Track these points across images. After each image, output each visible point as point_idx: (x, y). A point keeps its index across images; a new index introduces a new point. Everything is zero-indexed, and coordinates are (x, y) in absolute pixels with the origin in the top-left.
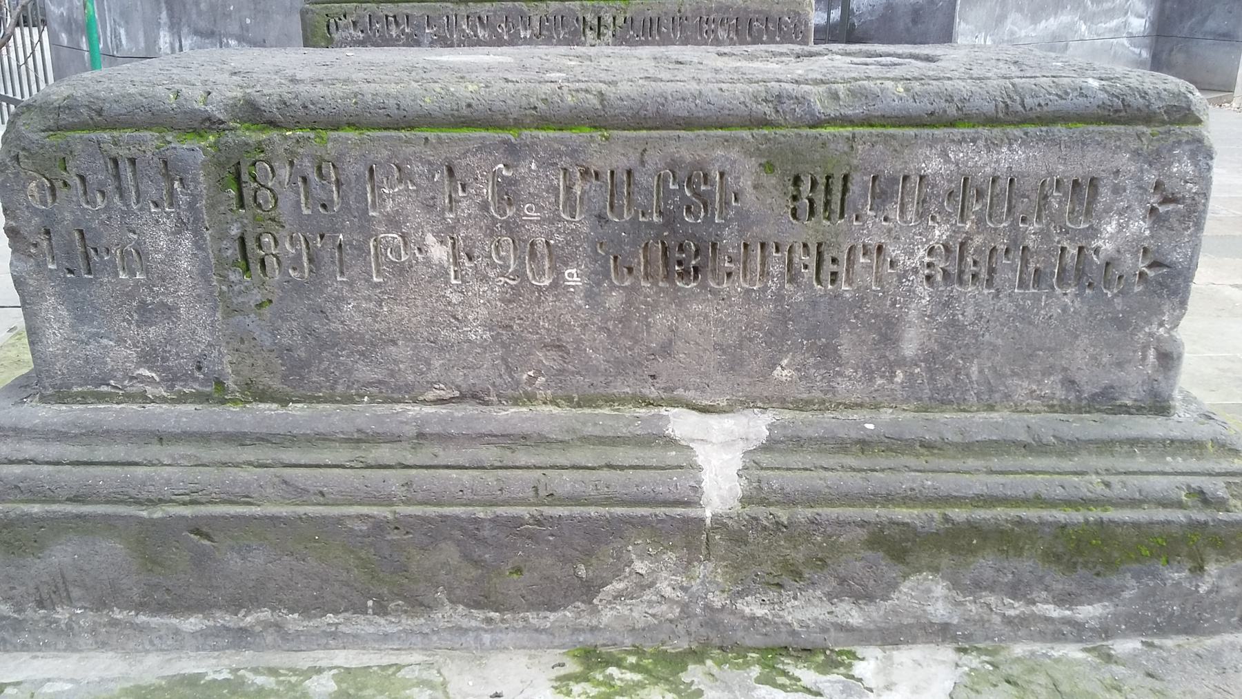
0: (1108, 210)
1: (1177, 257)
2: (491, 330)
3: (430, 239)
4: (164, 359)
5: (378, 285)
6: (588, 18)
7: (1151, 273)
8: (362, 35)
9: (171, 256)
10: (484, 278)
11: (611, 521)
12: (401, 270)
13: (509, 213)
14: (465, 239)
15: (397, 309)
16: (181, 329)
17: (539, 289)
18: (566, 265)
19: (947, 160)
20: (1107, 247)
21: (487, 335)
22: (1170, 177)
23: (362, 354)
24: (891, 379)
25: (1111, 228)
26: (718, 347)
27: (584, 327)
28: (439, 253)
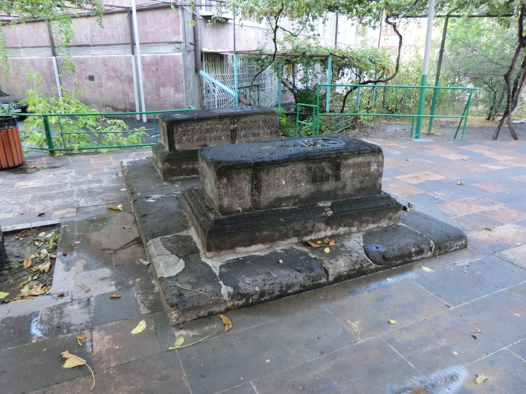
1: (381, 171)
3: (283, 181)
7: (378, 174)
9: (245, 188)
10: (290, 186)
13: (294, 175)
25: (372, 168)
28: (284, 183)
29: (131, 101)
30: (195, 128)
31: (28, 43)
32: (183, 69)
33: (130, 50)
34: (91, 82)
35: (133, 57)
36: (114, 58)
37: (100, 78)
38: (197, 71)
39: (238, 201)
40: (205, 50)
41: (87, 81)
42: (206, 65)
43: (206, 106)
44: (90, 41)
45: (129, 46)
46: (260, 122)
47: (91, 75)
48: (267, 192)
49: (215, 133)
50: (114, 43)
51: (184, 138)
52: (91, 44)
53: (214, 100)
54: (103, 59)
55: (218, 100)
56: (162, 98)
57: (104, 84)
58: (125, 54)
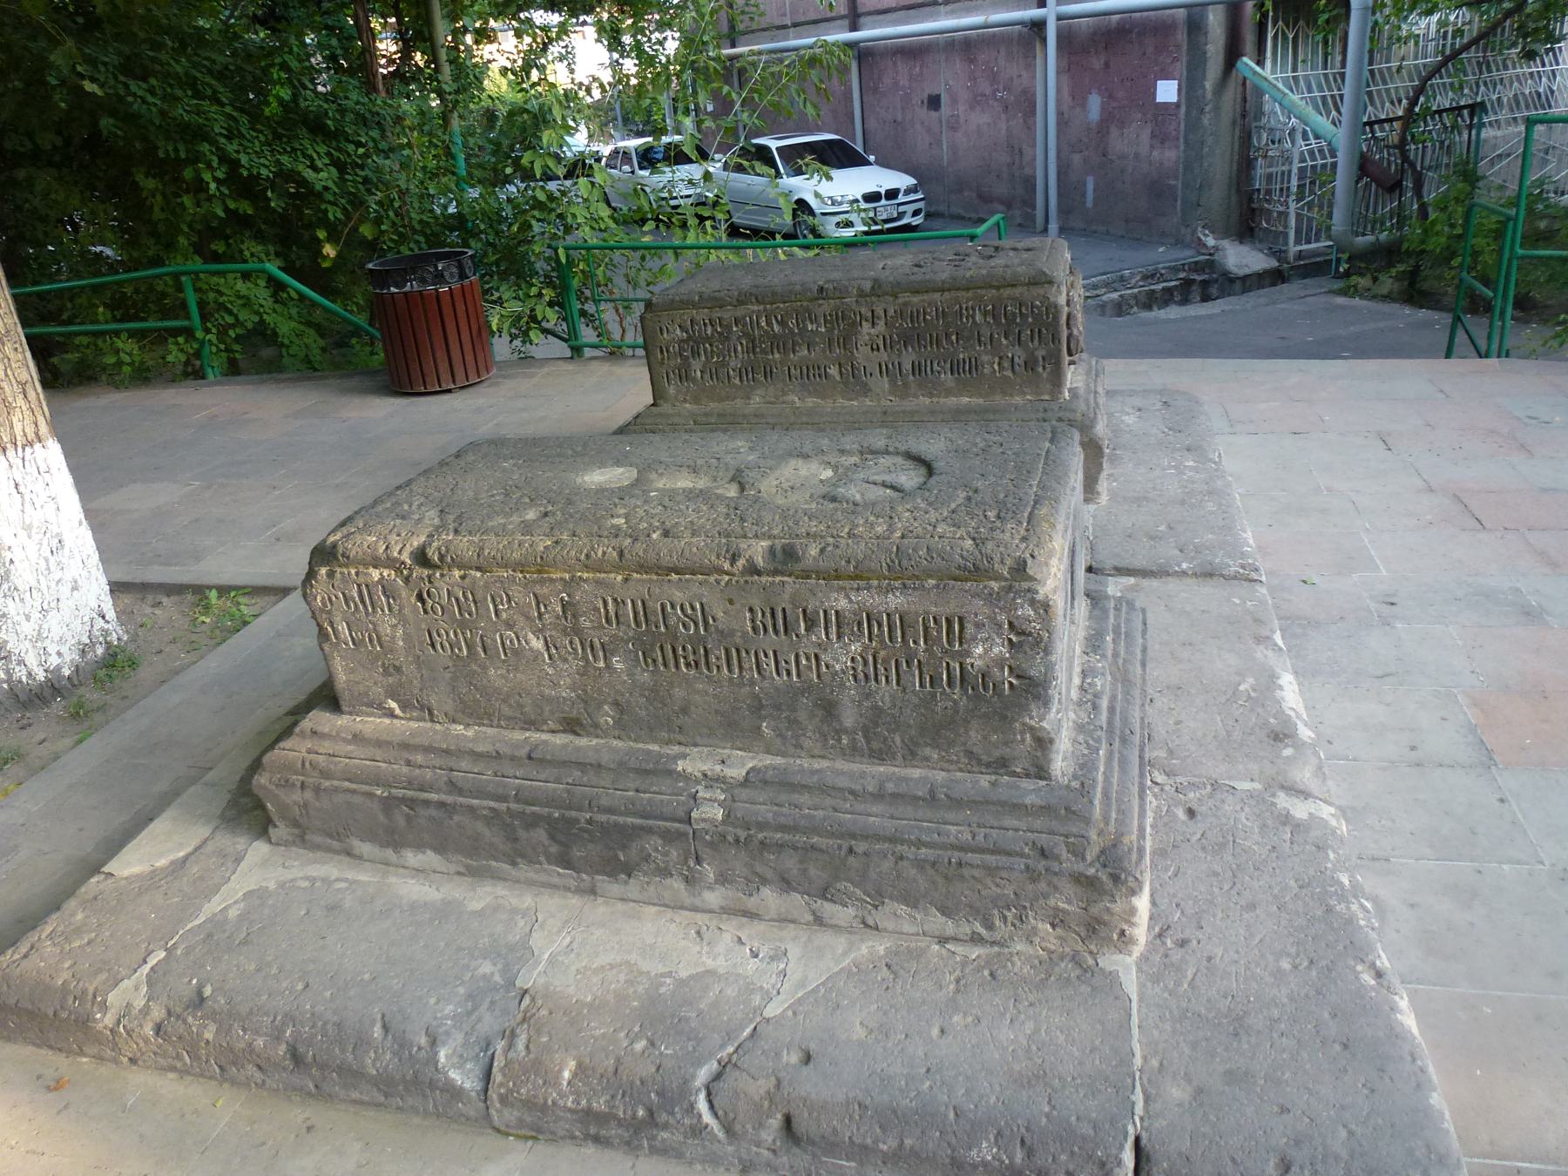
0: (974, 639)
3: (530, 636)
5: (504, 661)
10: (565, 660)
11: (634, 827)
12: (516, 653)
19: (851, 601)
20: (978, 663)
22: (1018, 617)
24: (839, 740)
25: (979, 650)
28: (537, 644)
29: (1027, 171)
30: (730, 331)
34: (934, 114)
37: (954, 101)
41: (923, 113)
42: (1275, 37)
43: (1259, 190)
46: (978, 318)
47: (936, 92)
53: (1285, 168)
57: (962, 120)
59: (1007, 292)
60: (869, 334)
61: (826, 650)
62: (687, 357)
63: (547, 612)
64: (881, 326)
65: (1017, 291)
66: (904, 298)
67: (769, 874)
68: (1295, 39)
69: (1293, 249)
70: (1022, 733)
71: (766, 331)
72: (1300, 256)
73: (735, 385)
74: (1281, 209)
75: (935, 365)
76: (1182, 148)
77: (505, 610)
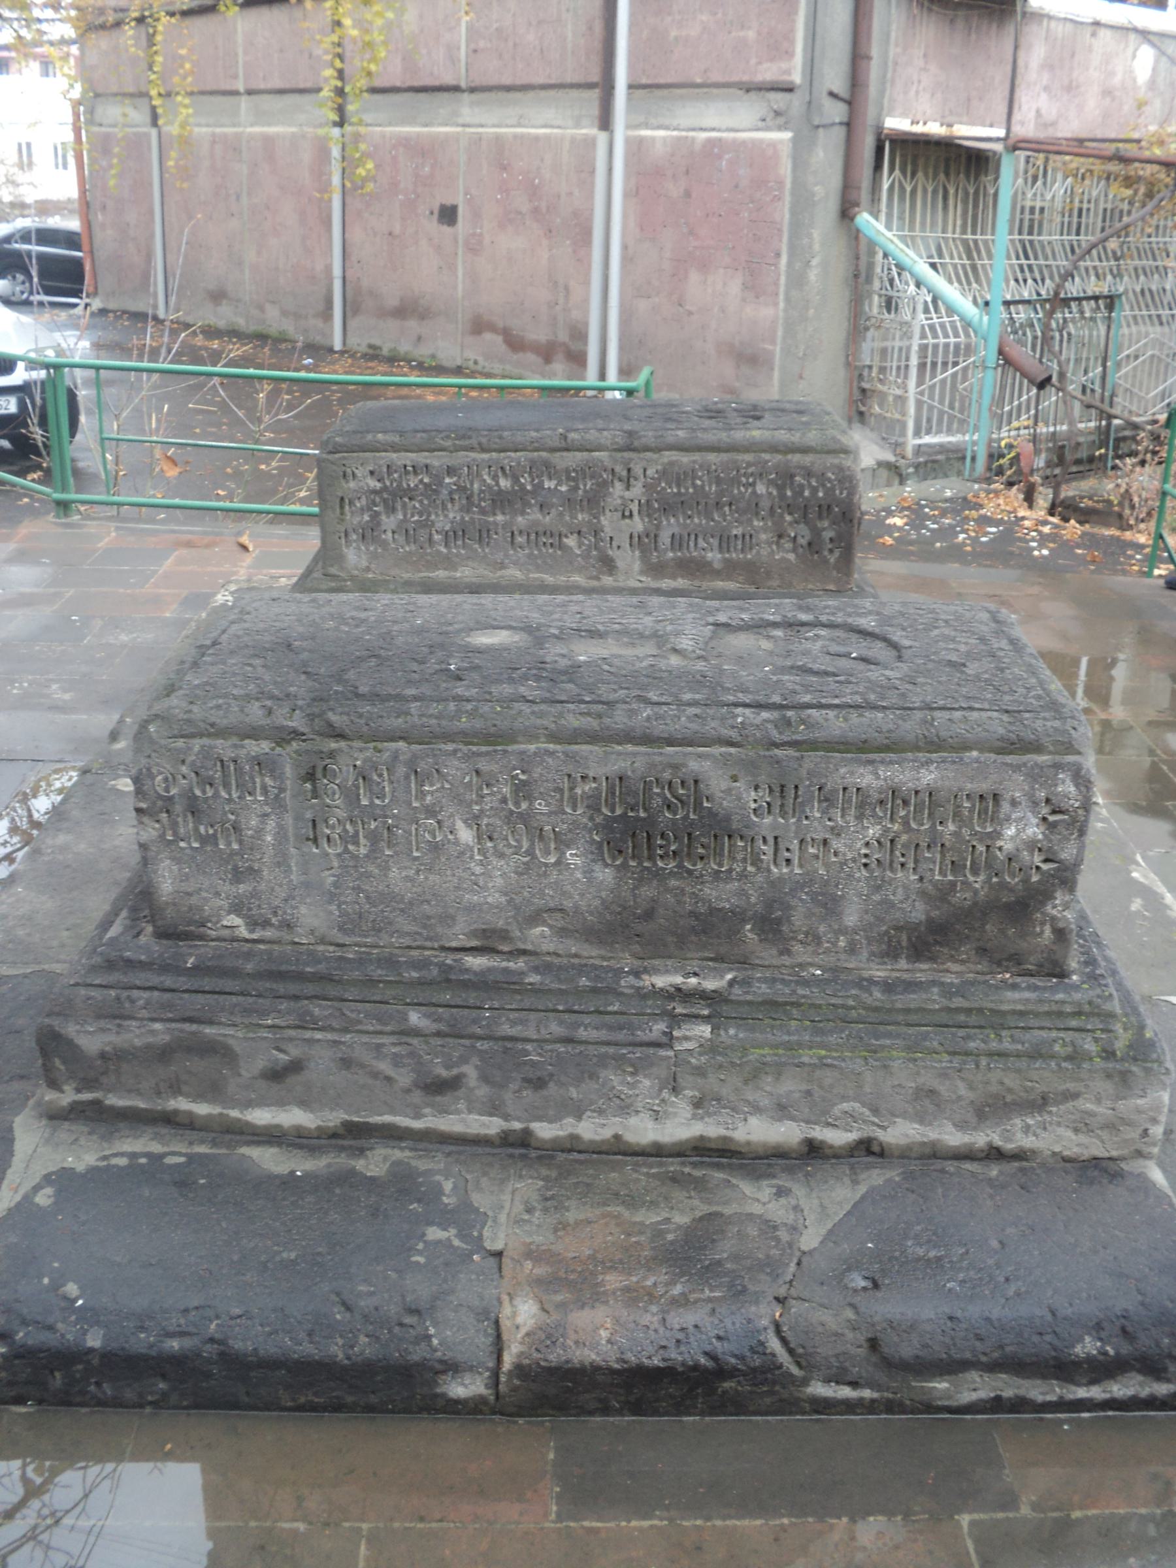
0: (1008, 819)
1: (1067, 853)
2: (506, 894)
3: (460, 825)
4: (250, 909)
5: (416, 858)
6: (618, 469)
7: (1045, 867)
8: (379, 485)
9: (259, 832)
10: (501, 856)
12: (435, 848)
13: (524, 806)
14: (487, 825)
15: (431, 877)
16: (263, 886)
17: (546, 865)
18: (569, 847)
19: (878, 778)
21: (503, 899)
22: (1057, 795)
23: (402, 910)
25: (1011, 831)
26: (692, 914)
27: (582, 895)
28: (466, 835)
29: (575, 314)
30: (440, 483)
31: (264, 78)
32: (787, 198)
33: (595, 111)
34: (446, 229)
35: (602, 137)
36: (537, 139)
37: (477, 215)
38: (846, 213)
39: (226, 888)
40: (896, 123)
41: (432, 226)
43: (870, 367)
44: (463, 71)
45: (595, 94)
47: (449, 202)
48: (372, 868)
49: (534, 515)
50: (541, 80)
51: (389, 522)
52: (463, 85)
53: (905, 343)
54: (499, 142)
55: (923, 348)
56: (690, 313)
57: (487, 240)
58: (577, 125)
59: (796, 458)
60: (622, 497)
61: (839, 835)
62: (377, 514)
63: (492, 794)
64: (637, 490)
65: (807, 459)
66: (668, 456)
67: (765, 1102)
68: (914, 192)
69: (912, 442)
70: (1043, 923)
71: (490, 487)
72: (918, 449)
73: (439, 552)
74: (898, 392)
75: (700, 540)
76: (782, 305)
77: (432, 793)
